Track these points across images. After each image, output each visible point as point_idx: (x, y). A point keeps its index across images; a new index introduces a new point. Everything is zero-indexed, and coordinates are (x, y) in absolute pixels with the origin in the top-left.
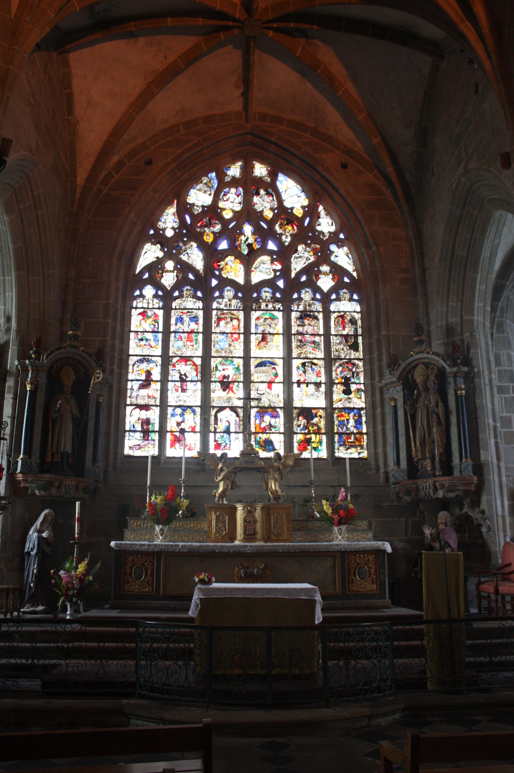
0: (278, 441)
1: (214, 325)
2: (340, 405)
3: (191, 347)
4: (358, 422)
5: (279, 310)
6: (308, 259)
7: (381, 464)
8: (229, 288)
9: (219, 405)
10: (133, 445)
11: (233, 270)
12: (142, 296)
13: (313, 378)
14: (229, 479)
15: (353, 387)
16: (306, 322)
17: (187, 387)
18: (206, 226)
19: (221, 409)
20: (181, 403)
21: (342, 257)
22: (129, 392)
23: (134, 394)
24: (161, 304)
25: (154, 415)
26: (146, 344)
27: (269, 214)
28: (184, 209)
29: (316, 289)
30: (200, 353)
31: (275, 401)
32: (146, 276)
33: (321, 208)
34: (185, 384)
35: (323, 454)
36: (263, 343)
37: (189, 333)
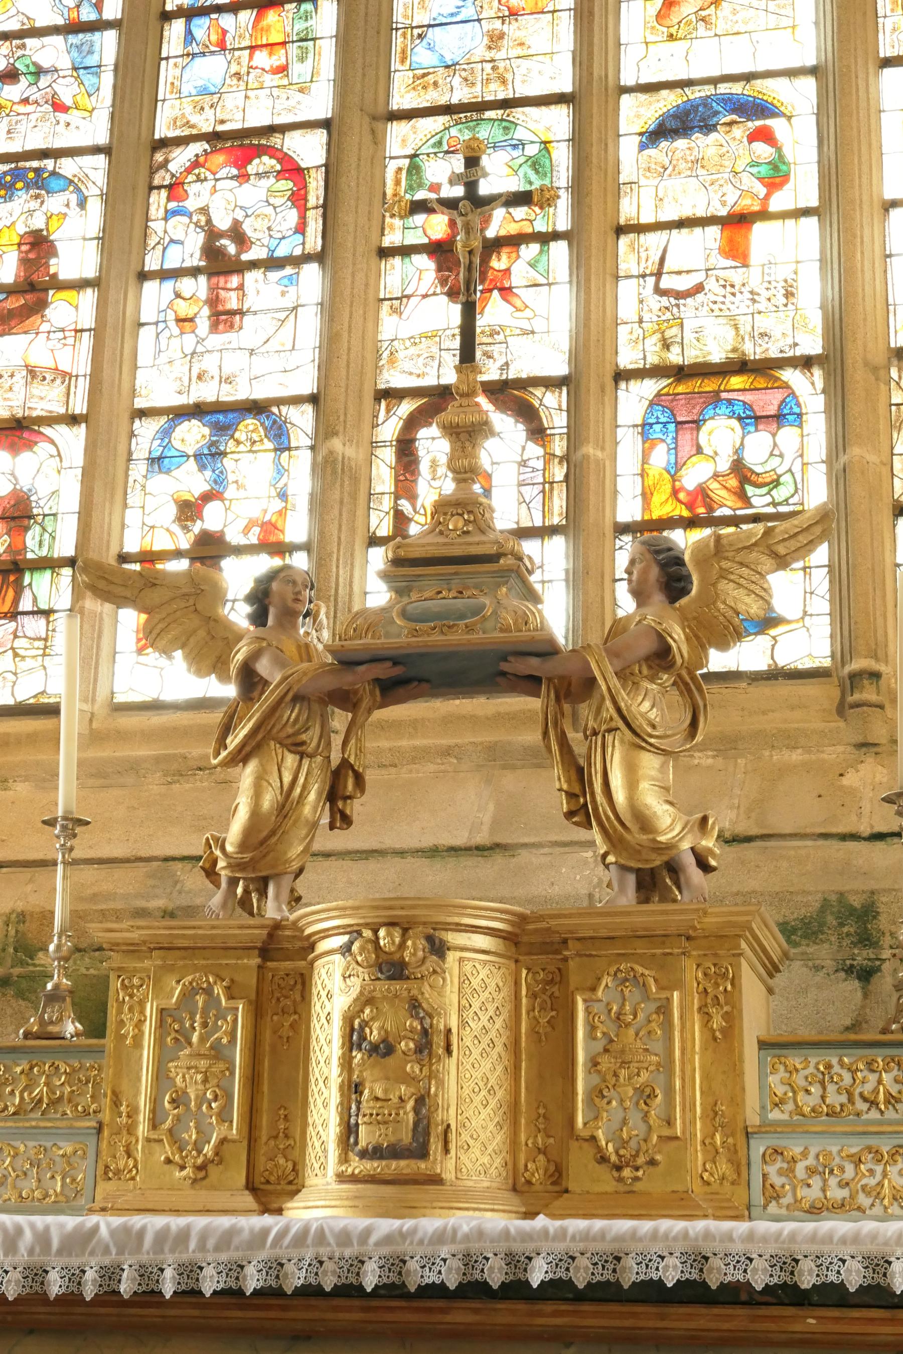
3: (270, 80)
9: (430, 381)
14: (297, 748)
17: (241, 299)
20: (207, 393)
26: (33, 93)
30: (320, 103)
31: (763, 323)
34: (234, 281)
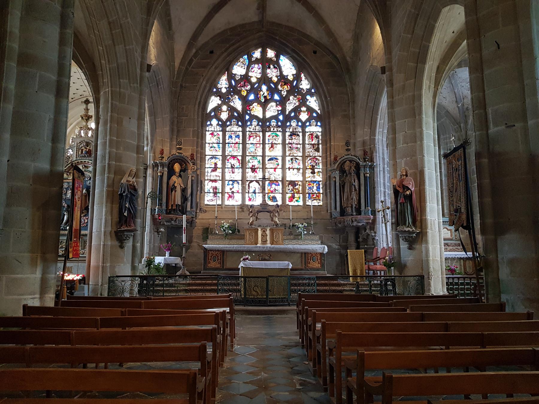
0: (279, 197)
1: (247, 140)
2: (309, 179)
4: (318, 188)
5: (280, 131)
6: (295, 104)
7: (329, 209)
8: (254, 120)
10: (209, 199)
11: (257, 110)
12: (211, 125)
13: (296, 166)
15: (316, 170)
16: (293, 137)
18: (243, 86)
19: (251, 181)
20: (232, 179)
21: (313, 102)
22: (206, 173)
23: (209, 175)
24: (221, 129)
25: (219, 185)
27: (275, 79)
28: (231, 77)
29: (299, 120)
30: (241, 154)
32: (213, 114)
33: (302, 75)
35: (301, 203)
36: (271, 149)
37: (235, 144)
